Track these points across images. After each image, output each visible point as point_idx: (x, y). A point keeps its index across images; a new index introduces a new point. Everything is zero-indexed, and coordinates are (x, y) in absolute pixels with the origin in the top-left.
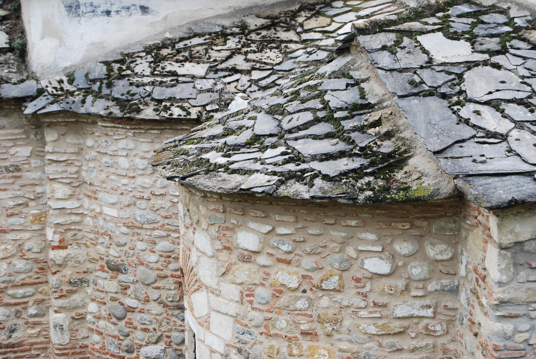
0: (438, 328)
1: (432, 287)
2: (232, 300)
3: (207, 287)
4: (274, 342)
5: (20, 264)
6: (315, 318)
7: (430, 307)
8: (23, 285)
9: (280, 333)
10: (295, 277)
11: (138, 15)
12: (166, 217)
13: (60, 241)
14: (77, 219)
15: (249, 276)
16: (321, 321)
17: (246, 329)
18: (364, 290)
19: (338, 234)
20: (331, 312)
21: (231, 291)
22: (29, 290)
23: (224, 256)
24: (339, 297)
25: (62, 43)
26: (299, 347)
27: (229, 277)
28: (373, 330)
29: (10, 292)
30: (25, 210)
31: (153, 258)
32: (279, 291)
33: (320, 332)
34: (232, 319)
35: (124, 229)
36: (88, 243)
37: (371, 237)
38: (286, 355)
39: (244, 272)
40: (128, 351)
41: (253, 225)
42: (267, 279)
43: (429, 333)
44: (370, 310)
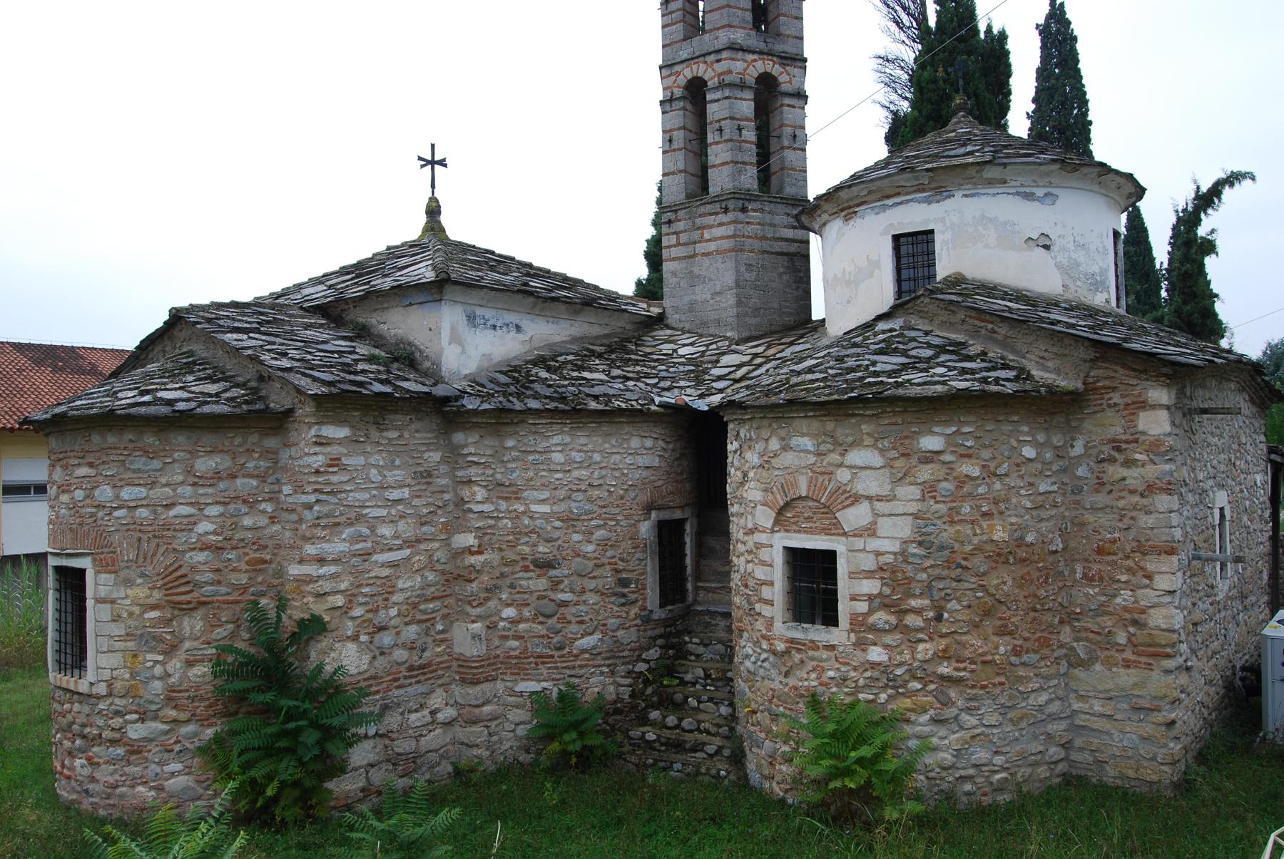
1: (1055, 468)
3: (869, 498)
5: (431, 577)
8: (433, 598)
11: (513, 333)
12: (604, 507)
13: (479, 546)
14: (491, 522)
16: (996, 502)
19: (1007, 428)
20: (1003, 493)
21: (909, 492)
22: (438, 603)
23: (898, 464)
25: (463, 351)
26: (981, 527)
27: (908, 479)
28: (1029, 505)
29: (422, 607)
30: (435, 519)
31: (590, 548)
32: (963, 480)
35: (558, 524)
36: (504, 547)
37: (1026, 429)
39: (925, 473)
40: (559, 649)
41: (936, 429)
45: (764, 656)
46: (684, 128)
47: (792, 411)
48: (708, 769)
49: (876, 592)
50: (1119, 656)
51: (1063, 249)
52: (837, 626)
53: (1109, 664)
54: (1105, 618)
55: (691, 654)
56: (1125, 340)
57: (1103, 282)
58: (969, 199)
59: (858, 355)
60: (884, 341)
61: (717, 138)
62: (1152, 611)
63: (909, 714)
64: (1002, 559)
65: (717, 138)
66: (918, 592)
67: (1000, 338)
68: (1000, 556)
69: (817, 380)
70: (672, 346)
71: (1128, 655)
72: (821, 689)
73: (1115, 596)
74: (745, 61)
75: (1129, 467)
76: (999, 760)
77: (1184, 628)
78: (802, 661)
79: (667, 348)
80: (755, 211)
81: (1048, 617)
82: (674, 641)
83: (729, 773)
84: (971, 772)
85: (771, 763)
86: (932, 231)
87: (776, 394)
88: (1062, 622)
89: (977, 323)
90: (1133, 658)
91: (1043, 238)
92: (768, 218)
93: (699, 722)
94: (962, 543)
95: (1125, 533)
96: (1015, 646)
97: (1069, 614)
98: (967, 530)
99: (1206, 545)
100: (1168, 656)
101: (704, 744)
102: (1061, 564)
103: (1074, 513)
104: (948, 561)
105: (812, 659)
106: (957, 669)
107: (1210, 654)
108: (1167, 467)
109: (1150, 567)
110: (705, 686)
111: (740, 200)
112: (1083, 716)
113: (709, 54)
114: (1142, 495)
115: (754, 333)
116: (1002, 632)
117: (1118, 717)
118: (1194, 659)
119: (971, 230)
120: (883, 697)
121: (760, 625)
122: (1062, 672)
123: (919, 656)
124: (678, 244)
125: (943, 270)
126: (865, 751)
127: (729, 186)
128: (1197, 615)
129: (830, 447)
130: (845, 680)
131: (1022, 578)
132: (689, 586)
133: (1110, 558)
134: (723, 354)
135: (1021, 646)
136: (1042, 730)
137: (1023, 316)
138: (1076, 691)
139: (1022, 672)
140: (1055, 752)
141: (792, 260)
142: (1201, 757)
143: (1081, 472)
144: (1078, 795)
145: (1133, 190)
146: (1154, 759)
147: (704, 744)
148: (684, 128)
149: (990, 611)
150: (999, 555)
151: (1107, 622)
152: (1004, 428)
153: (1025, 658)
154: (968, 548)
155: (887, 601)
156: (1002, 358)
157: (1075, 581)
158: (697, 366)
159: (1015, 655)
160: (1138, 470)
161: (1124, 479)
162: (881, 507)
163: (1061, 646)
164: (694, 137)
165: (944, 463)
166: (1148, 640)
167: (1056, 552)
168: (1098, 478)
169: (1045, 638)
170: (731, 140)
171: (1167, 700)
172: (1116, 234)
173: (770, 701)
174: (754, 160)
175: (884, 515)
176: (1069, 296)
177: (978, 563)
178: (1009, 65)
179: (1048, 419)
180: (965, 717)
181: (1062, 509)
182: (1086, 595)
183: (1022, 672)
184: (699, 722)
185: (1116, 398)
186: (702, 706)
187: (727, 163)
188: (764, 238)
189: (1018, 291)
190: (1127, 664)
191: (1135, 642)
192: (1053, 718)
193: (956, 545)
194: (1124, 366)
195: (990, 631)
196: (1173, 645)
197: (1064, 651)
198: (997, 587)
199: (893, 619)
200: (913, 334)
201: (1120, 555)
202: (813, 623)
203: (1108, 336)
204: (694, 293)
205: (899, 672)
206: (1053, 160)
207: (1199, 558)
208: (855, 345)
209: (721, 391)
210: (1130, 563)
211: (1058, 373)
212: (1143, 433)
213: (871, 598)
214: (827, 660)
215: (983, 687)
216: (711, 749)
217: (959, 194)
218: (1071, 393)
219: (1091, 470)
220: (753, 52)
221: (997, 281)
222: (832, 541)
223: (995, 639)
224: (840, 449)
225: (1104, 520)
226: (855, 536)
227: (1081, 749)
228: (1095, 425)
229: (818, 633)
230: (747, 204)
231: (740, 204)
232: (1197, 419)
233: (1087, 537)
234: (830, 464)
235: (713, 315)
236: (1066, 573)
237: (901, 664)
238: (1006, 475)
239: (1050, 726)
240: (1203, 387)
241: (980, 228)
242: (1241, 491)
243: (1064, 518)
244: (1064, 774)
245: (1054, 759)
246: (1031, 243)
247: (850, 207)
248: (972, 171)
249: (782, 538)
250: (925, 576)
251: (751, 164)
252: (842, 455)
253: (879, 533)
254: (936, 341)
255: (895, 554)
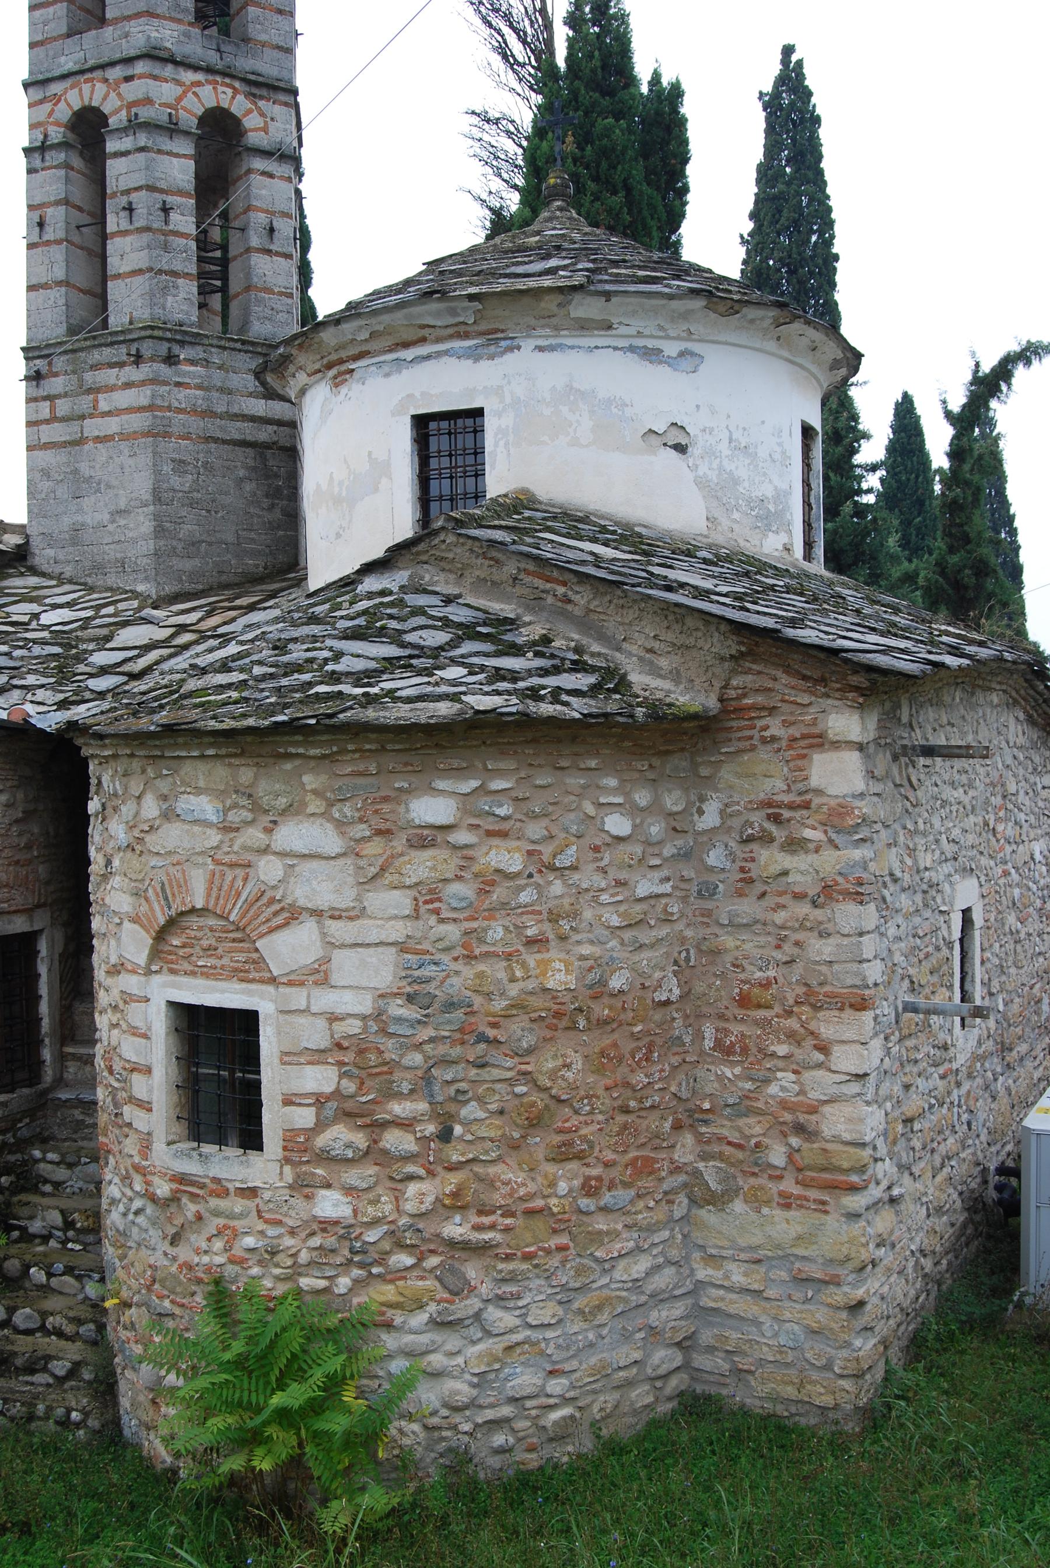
0: (675, 910)
1: (668, 851)
2: (395, 917)
4: (481, 967)
6: (545, 916)
7: (668, 879)
9: (492, 949)
10: (517, 855)
15: (433, 868)
16: (554, 918)
17: (428, 957)
18: (602, 864)
19: (576, 781)
20: (566, 901)
23: (375, 848)
24: (576, 876)
26: (524, 965)
27: (388, 878)
28: (615, 921)
32: (488, 882)
33: (551, 937)
34: (393, 950)
37: (612, 782)
38: (505, 981)
39: (421, 866)
41: (441, 784)
42: (469, 867)
43: (667, 919)
44: (611, 891)
45: (138, 1204)
46: (66, 202)
47: (176, 746)
48: (49, 1409)
49: (328, 1088)
50: (774, 1188)
51: (710, 453)
52: (260, 1148)
53: (757, 1200)
54: (752, 1120)
55: (46, 1181)
56: (793, 623)
57: (780, 514)
58: (546, 355)
59: (315, 638)
60: (365, 612)
61: (124, 225)
62: (827, 1109)
63: (390, 1313)
64: (564, 1023)
65: (124, 225)
66: (405, 1087)
67: (577, 612)
68: (560, 1017)
69: (229, 686)
70: (35, 608)
71: (789, 1185)
72: (231, 1270)
73: (767, 1081)
74: (178, 82)
75: (793, 852)
76: (557, 1386)
77: (885, 1134)
78: (199, 1218)
79: (20, 611)
80: (192, 362)
81: (652, 1122)
82: (12, 1158)
83: (86, 1415)
84: (506, 1411)
85: (154, 1402)
86: (479, 412)
87: (153, 711)
88: (677, 1127)
89: (538, 582)
90: (796, 1190)
91: (674, 431)
92: (218, 377)
93: (44, 1314)
94: (488, 996)
95: (783, 969)
96: (588, 1179)
97: (691, 1112)
98: (498, 971)
99: (935, 979)
100: (854, 1189)
101: (48, 1358)
102: (678, 1023)
103: (703, 932)
104: (461, 1030)
105: (217, 1213)
106: (478, 1228)
107: (938, 1161)
108: (857, 854)
109: (827, 1031)
110: (64, 1243)
111: (168, 341)
112: (714, 1292)
113: (112, 64)
114: (815, 904)
115: (188, 587)
116: (562, 1154)
117: (770, 1293)
118: (907, 1179)
119: (547, 412)
120: (344, 1283)
121: (131, 1146)
122: (677, 1215)
123: (409, 1207)
124: (53, 419)
125: (499, 480)
126: (293, 1396)
127: (144, 315)
128: (914, 1103)
129: (250, 816)
130: (273, 1254)
131: (602, 1054)
132: (47, 1054)
133: (761, 1013)
134: (125, 624)
135: (599, 1179)
136: (640, 1321)
137: (622, 571)
138: (702, 1248)
139: (601, 1224)
140: (664, 1358)
141: (264, 459)
142: (917, 1347)
143: (715, 858)
144: (704, 1434)
145: (839, 355)
146: (828, 1367)
147: (48, 1358)
148: (66, 202)
149: (539, 1117)
150: (558, 1015)
151: (754, 1127)
152: (570, 781)
153: (607, 1198)
154: (499, 1005)
155: (349, 1105)
156: (578, 650)
157: (702, 1053)
158: (68, 646)
159: (588, 1195)
160: (811, 858)
161: (785, 873)
162: (338, 929)
163: (677, 1170)
164: (87, 220)
165: (455, 847)
166: (821, 1161)
167: (667, 1003)
168: (742, 870)
169: (647, 1160)
170: (148, 229)
171: (850, 1266)
172: (807, 431)
173: (149, 1288)
174: (194, 270)
175: (343, 946)
176: (718, 538)
177: (520, 1031)
178: (685, 142)
179: (656, 762)
180: (493, 1313)
181: (680, 926)
182: (720, 1078)
183: (601, 1224)
184: (44, 1314)
185: (775, 728)
186: (54, 1282)
187: (139, 272)
188: (209, 413)
189: (628, 526)
190: (787, 1202)
191: (801, 1163)
192: (659, 1298)
193: (478, 1001)
194: (788, 670)
195: (540, 1154)
196: (862, 1169)
197: (682, 1178)
198: (553, 1074)
199: (360, 1140)
200: (421, 600)
201: (778, 1009)
202: (221, 1141)
203: (761, 616)
204: (80, 510)
205: (371, 1236)
206: (692, 291)
207: (915, 1010)
208: (314, 620)
209: (101, 695)
210: (792, 1023)
211: (677, 681)
212: (819, 792)
213: (319, 1101)
214: (242, 1216)
215: (528, 1257)
216: (60, 1368)
217: (528, 345)
218: (695, 716)
219: (731, 856)
220: (196, 68)
221: (592, 507)
222: (250, 993)
223: (551, 1168)
224: (265, 820)
225: (751, 945)
226: (290, 984)
227: (711, 1349)
228: (738, 775)
229: (226, 1164)
230: (176, 349)
231: (163, 348)
232: (922, 761)
233: (723, 976)
234: (245, 848)
235: (113, 553)
236: (687, 1039)
237: (375, 1222)
238: (574, 868)
239: (655, 1314)
240: (939, 704)
241: (565, 409)
242: (1006, 874)
243: (683, 940)
244: (681, 1394)
245: (661, 1371)
246: (654, 440)
247: (341, 362)
248: (550, 303)
249: (165, 985)
250: (417, 1058)
251: (186, 275)
252: (268, 831)
253: (335, 979)
254: (459, 614)
255: (364, 1018)
